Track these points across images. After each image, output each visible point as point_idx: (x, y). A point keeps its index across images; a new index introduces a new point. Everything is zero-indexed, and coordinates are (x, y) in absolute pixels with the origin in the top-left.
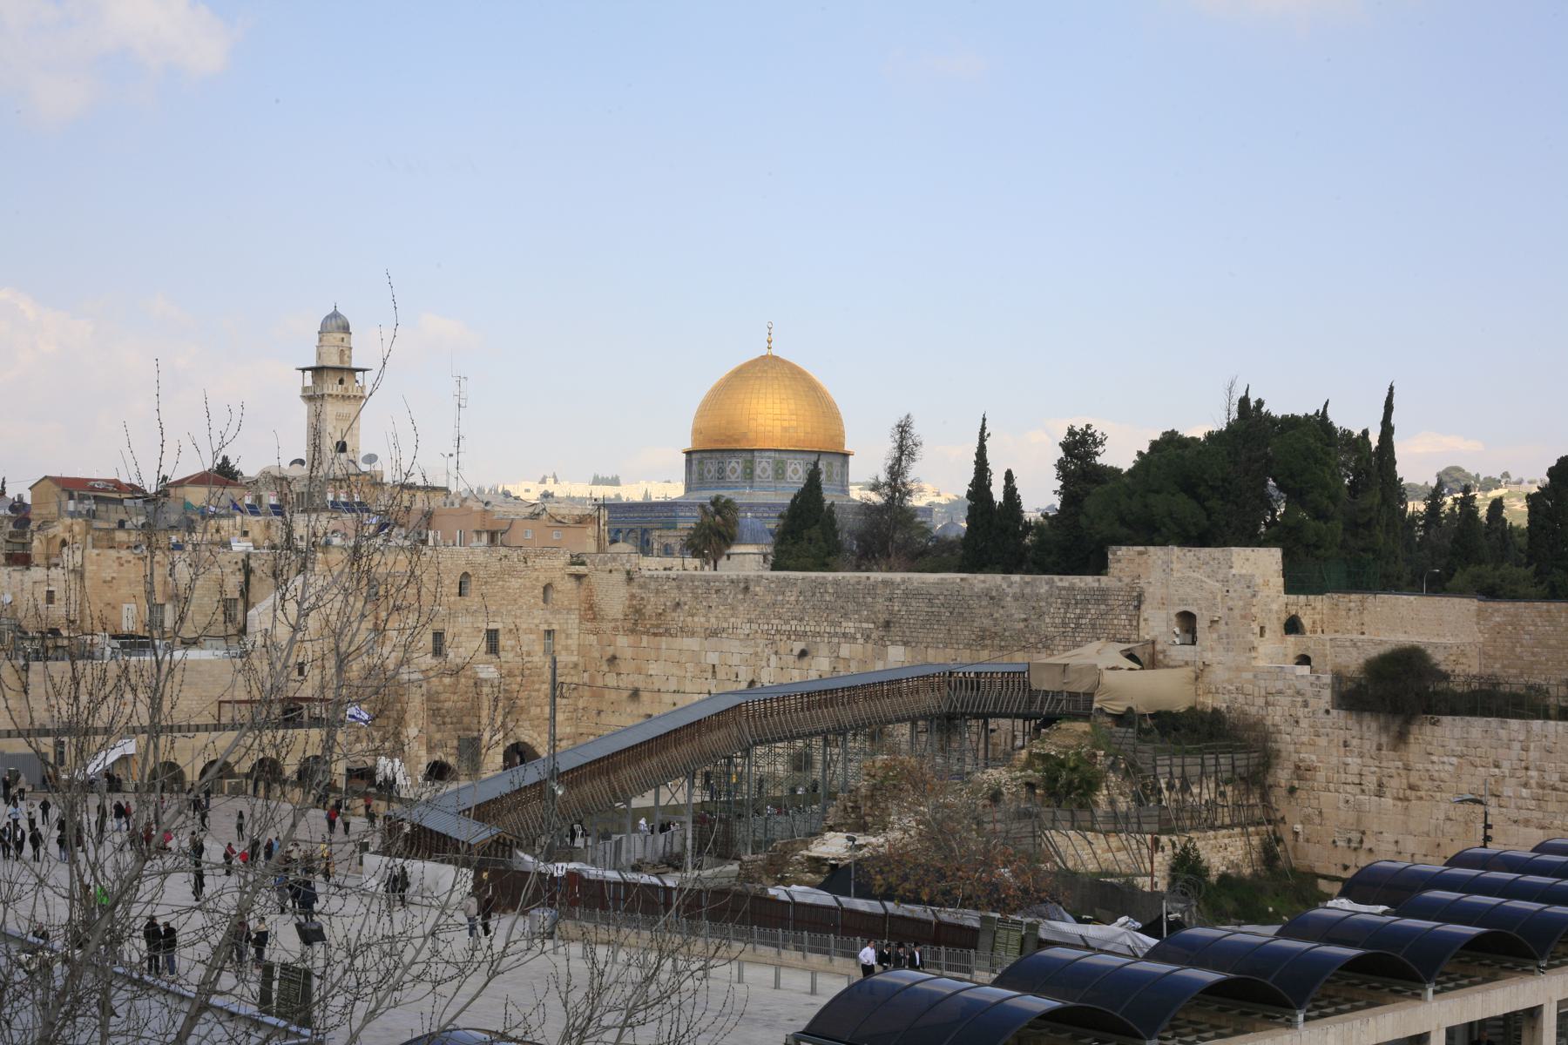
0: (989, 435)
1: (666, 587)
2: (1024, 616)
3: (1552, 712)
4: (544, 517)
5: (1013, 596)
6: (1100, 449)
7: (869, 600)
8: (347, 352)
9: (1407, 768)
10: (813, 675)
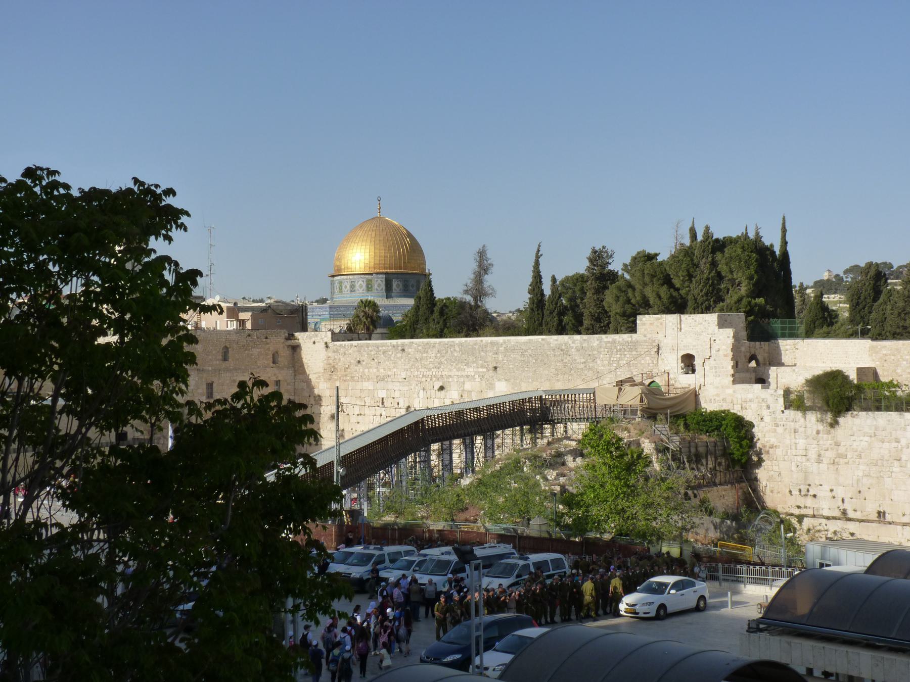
0: (541, 255)
1: (350, 351)
2: (583, 360)
4: (270, 311)
6: (610, 261)
7: (483, 354)
9: (838, 444)
10: (448, 402)
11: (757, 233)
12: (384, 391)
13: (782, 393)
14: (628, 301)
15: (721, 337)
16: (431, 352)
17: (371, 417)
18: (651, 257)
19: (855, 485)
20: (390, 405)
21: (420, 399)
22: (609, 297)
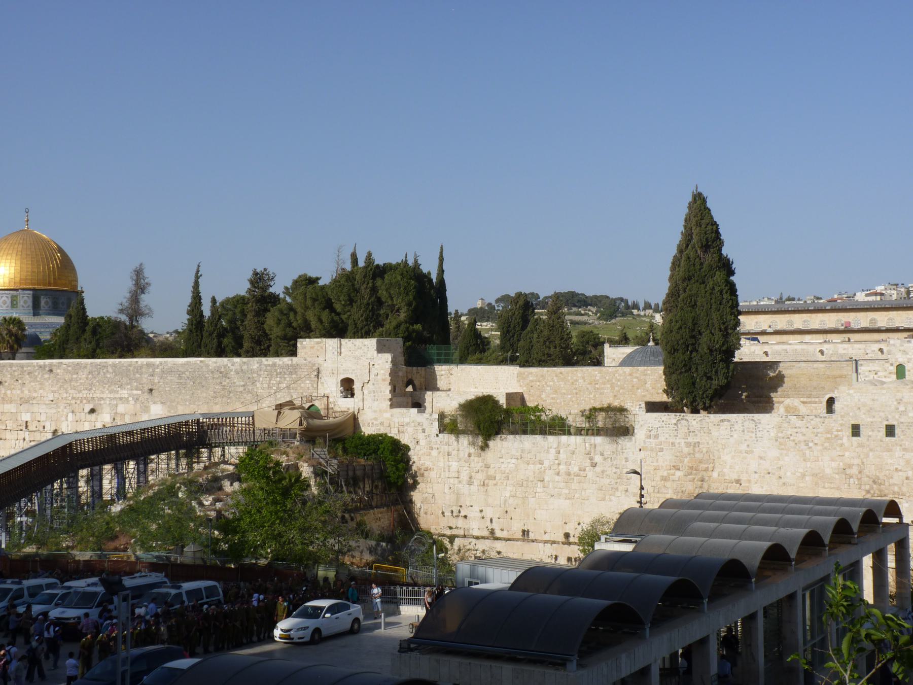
0: (201, 275)
2: (242, 383)
3: (572, 431)
5: (235, 371)
6: (272, 283)
7: (138, 376)
9: (487, 467)
10: (99, 425)
11: (416, 261)
12: (29, 415)
13: (437, 417)
14: (290, 325)
15: (380, 362)
16: (82, 373)
17: (13, 442)
18: (312, 281)
19: (503, 506)
20: (34, 429)
22: (270, 320)
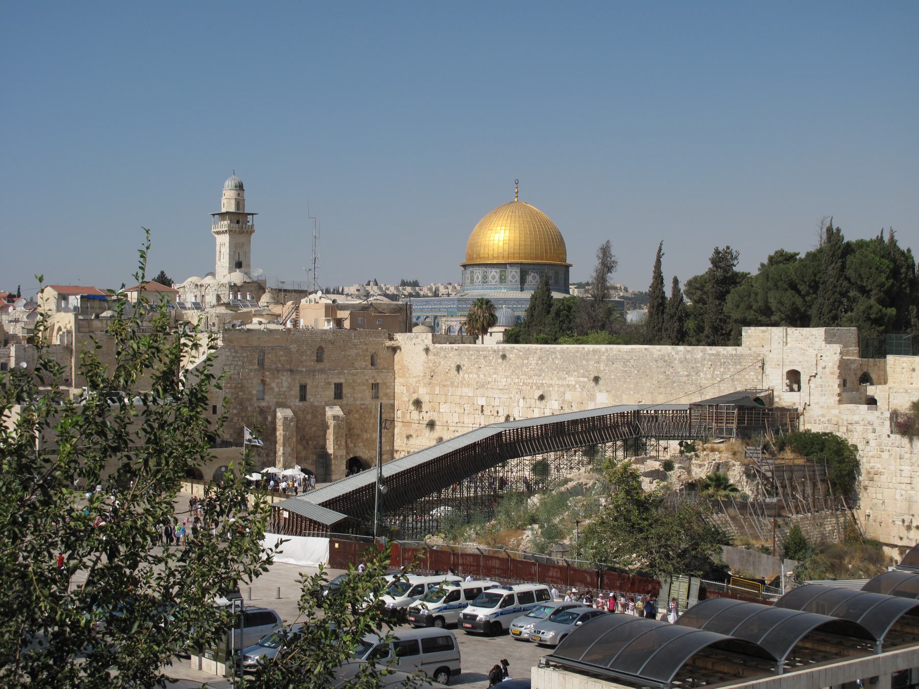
2: (686, 373)
4: (371, 309)
6: (735, 262)
7: (584, 362)
8: (241, 203)
10: (548, 413)
11: (892, 237)
14: (750, 307)
15: (828, 353)
21: (520, 408)
